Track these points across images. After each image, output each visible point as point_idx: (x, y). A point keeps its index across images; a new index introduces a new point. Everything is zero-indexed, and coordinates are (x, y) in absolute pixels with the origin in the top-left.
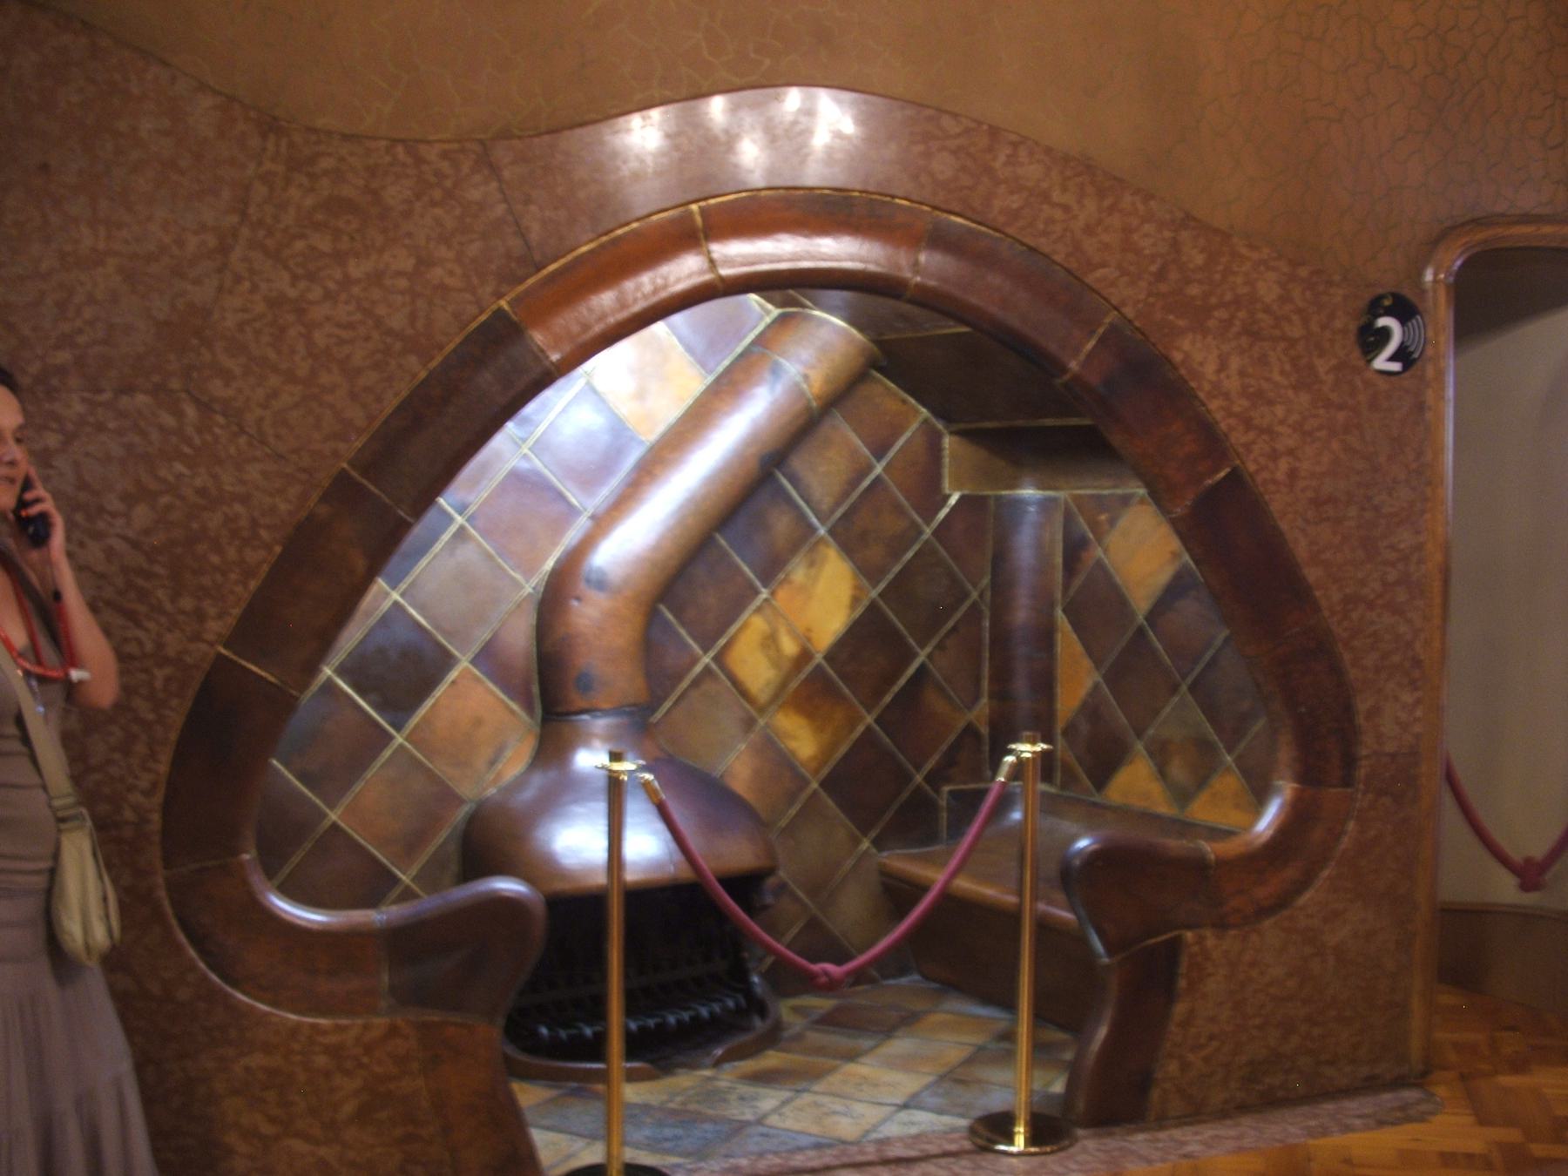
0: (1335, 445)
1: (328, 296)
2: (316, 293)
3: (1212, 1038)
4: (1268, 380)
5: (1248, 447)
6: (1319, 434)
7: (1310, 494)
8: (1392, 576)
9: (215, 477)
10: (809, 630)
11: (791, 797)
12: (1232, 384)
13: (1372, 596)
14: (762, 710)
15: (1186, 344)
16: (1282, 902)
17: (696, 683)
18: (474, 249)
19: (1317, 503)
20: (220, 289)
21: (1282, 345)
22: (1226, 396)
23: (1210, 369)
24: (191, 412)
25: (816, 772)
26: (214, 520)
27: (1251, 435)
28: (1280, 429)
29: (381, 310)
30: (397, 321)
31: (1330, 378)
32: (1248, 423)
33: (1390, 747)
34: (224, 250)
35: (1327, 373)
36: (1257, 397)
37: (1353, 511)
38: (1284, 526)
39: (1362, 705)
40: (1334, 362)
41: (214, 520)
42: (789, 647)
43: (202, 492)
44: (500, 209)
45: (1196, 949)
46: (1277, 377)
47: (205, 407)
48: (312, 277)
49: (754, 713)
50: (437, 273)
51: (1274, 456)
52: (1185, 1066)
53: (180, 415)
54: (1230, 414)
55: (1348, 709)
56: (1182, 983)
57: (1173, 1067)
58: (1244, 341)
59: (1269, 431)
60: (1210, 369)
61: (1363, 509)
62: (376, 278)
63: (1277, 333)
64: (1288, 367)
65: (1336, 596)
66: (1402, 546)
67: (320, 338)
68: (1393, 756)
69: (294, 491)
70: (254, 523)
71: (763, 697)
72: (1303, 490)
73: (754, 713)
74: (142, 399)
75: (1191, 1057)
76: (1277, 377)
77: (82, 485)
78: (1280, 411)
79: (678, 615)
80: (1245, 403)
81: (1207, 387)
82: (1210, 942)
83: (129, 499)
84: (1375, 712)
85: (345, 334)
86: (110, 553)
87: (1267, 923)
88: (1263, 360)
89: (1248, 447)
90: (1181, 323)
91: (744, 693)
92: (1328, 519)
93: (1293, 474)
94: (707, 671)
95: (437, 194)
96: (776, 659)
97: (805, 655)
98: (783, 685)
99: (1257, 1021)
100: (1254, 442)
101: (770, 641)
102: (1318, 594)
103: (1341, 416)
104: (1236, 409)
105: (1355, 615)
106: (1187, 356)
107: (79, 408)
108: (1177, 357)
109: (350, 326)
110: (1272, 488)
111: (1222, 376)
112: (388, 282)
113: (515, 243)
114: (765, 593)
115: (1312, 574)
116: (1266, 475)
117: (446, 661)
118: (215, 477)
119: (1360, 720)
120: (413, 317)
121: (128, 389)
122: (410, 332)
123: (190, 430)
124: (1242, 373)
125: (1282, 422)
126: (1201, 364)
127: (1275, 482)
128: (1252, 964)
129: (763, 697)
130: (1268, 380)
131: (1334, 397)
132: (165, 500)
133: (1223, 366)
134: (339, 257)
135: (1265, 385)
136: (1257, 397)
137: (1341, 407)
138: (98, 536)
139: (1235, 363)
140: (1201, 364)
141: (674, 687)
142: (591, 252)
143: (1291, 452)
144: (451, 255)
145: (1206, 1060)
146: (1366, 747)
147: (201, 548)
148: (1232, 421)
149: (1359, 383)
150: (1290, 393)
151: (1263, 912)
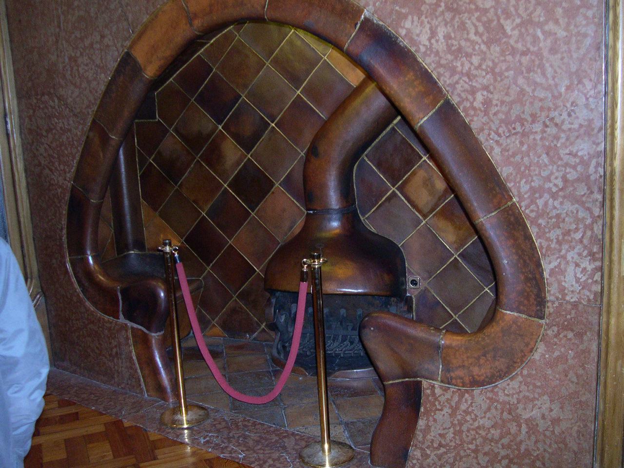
0: (521, 81)
1: (81, 54)
2: (78, 54)
3: (440, 445)
4: (467, 40)
5: (453, 86)
6: (506, 74)
7: (501, 116)
8: (572, 175)
9: (63, 123)
12: (440, 45)
13: (554, 190)
15: (408, 24)
16: (492, 379)
18: (114, 29)
19: (507, 122)
20: (58, 56)
21: (477, 14)
22: (437, 53)
23: (424, 39)
24: (56, 101)
26: (64, 138)
27: (457, 77)
28: (474, 72)
29: (94, 57)
30: (98, 62)
31: (516, 32)
32: (453, 71)
33: (571, 298)
34: (57, 42)
35: (513, 29)
36: (458, 52)
37: (538, 127)
38: (481, 138)
39: (548, 266)
40: (518, 21)
41: (64, 138)
43: (61, 128)
44: (120, 11)
45: (428, 391)
46: (472, 36)
47: (59, 98)
48: (77, 48)
50: (106, 41)
51: (473, 91)
52: (425, 456)
53: (54, 101)
54: (439, 65)
55: (539, 265)
56: (422, 409)
57: (417, 453)
58: (448, 16)
59: (468, 75)
60: (424, 39)
61: (547, 126)
62: (92, 45)
63: (473, 7)
64: (481, 29)
65: (525, 188)
66: (580, 154)
67: (81, 71)
68: (575, 305)
69: (81, 127)
70: (73, 138)
72: (495, 114)
74: (46, 97)
75: (428, 452)
76: (472, 36)
77: (38, 127)
78: (476, 60)
80: (449, 57)
81: (423, 49)
82: (438, 391)
83: (48, 131)
84: (558, 272)
85: (86, 68)
86: (46, 149)
87: (477, 391)
88: (463, 27)
89: (453, 86)
90: (403, 11)
92: (516, 134)
93: (487, 103)
95: (103, 8)
99: (472, 447)
100: (457, 83)
102: (510, 185)
103: (525, 60)
104: (443, 62)
105: (540, 202)
106: (409, 31)
107: (35, 101)
108: (403, 32)
109: (87, 65)
110: (472, 113)
111: (433, 41)
112: (95, 46)
113: (125, 23)
115: (504, 171)
116: (468, 105)
118: (63, 123)
119: (546, 275)
120: (101, 59)
121: (43, 94)
122: (102, 65)
123: (57, 107)
124: (447, 37)
125: (479, 67)
126: (418, 35)
127: (474, 109)
128: (466, 412)
130: (467, 40)
131: (519, 46)
132: (54, 131)
133: (433, 34)
134: (82, 39)
135: (463, 43)
136: (458, 52)
137: (524, 53)
138: (43, 144)
139: (441, 32)
140: (418, 35)
142: (150, 22)
143: (486, 88)
144: (109, 32)
145: (440, 457)
146: (552, 293)
147: (63, 148)
148: (441, 70)
149: (539, 33)
150: (483, 47)
151: (475, 383)
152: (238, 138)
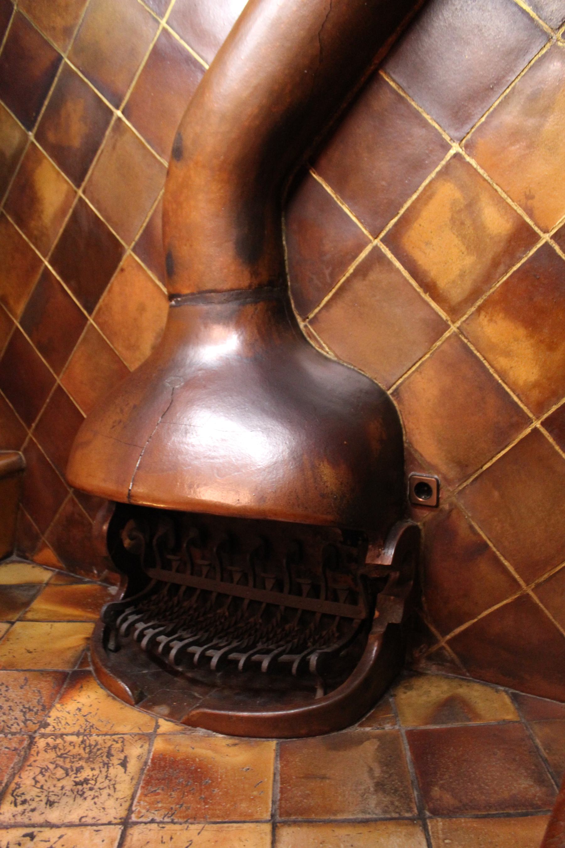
10: (529, 197)
11: (501, 437)
14: (455, 311)
17: (363, 271)
25: (540, 408)
42: (496, 223)
49: (443, 315)
71: (456, 295)
73: (443, 315)
79: (340, 185)
91: (430, 287)
94: (376, 255)
96: (475, 241)
97: (523, 235)
98: (488, 278)
101: (465, 216)
114: (455, 148)
117: (115, 251)
129: (456, 295)
141: (334, 279)
152: (60, 154)
